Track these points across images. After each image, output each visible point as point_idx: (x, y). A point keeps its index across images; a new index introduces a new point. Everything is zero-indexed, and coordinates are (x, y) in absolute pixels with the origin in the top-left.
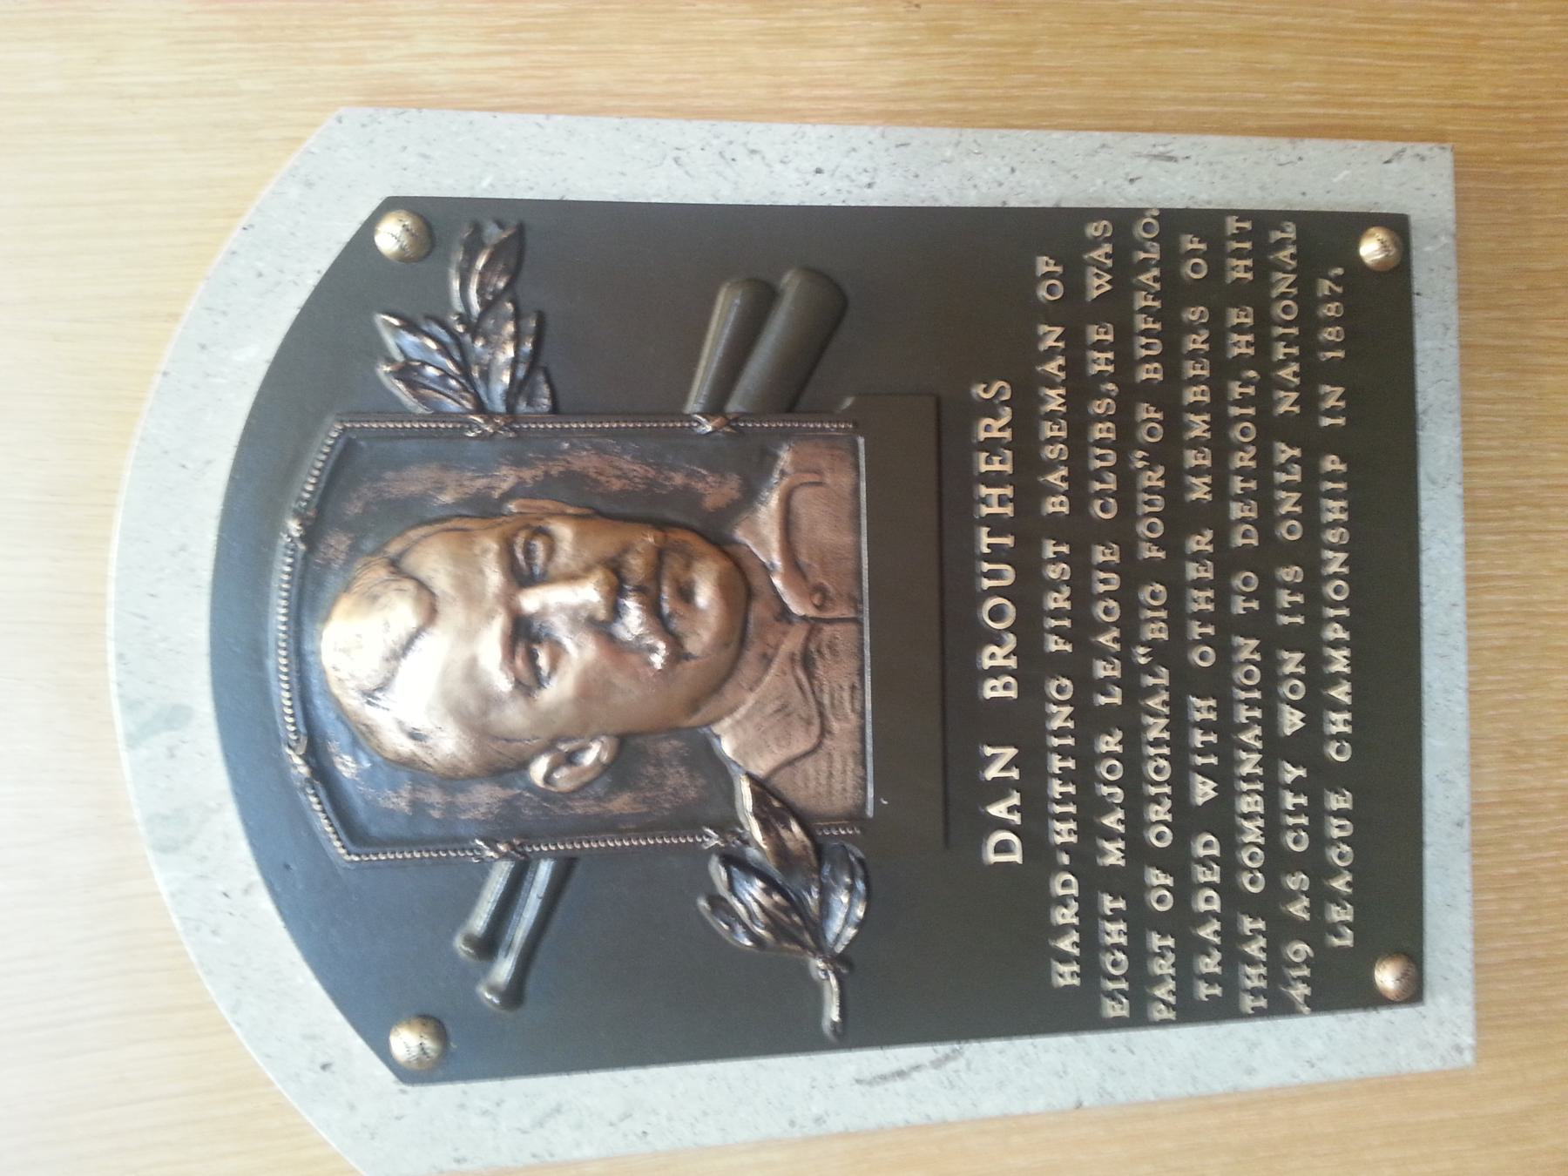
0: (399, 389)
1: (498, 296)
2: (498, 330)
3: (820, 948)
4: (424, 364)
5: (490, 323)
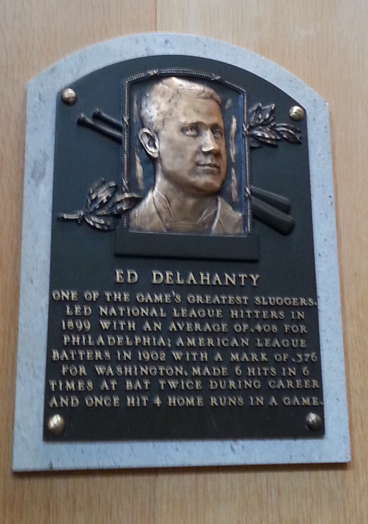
0: (255, 108)
1: (281, 136)
2: (273, 134)
4: (262, 114)
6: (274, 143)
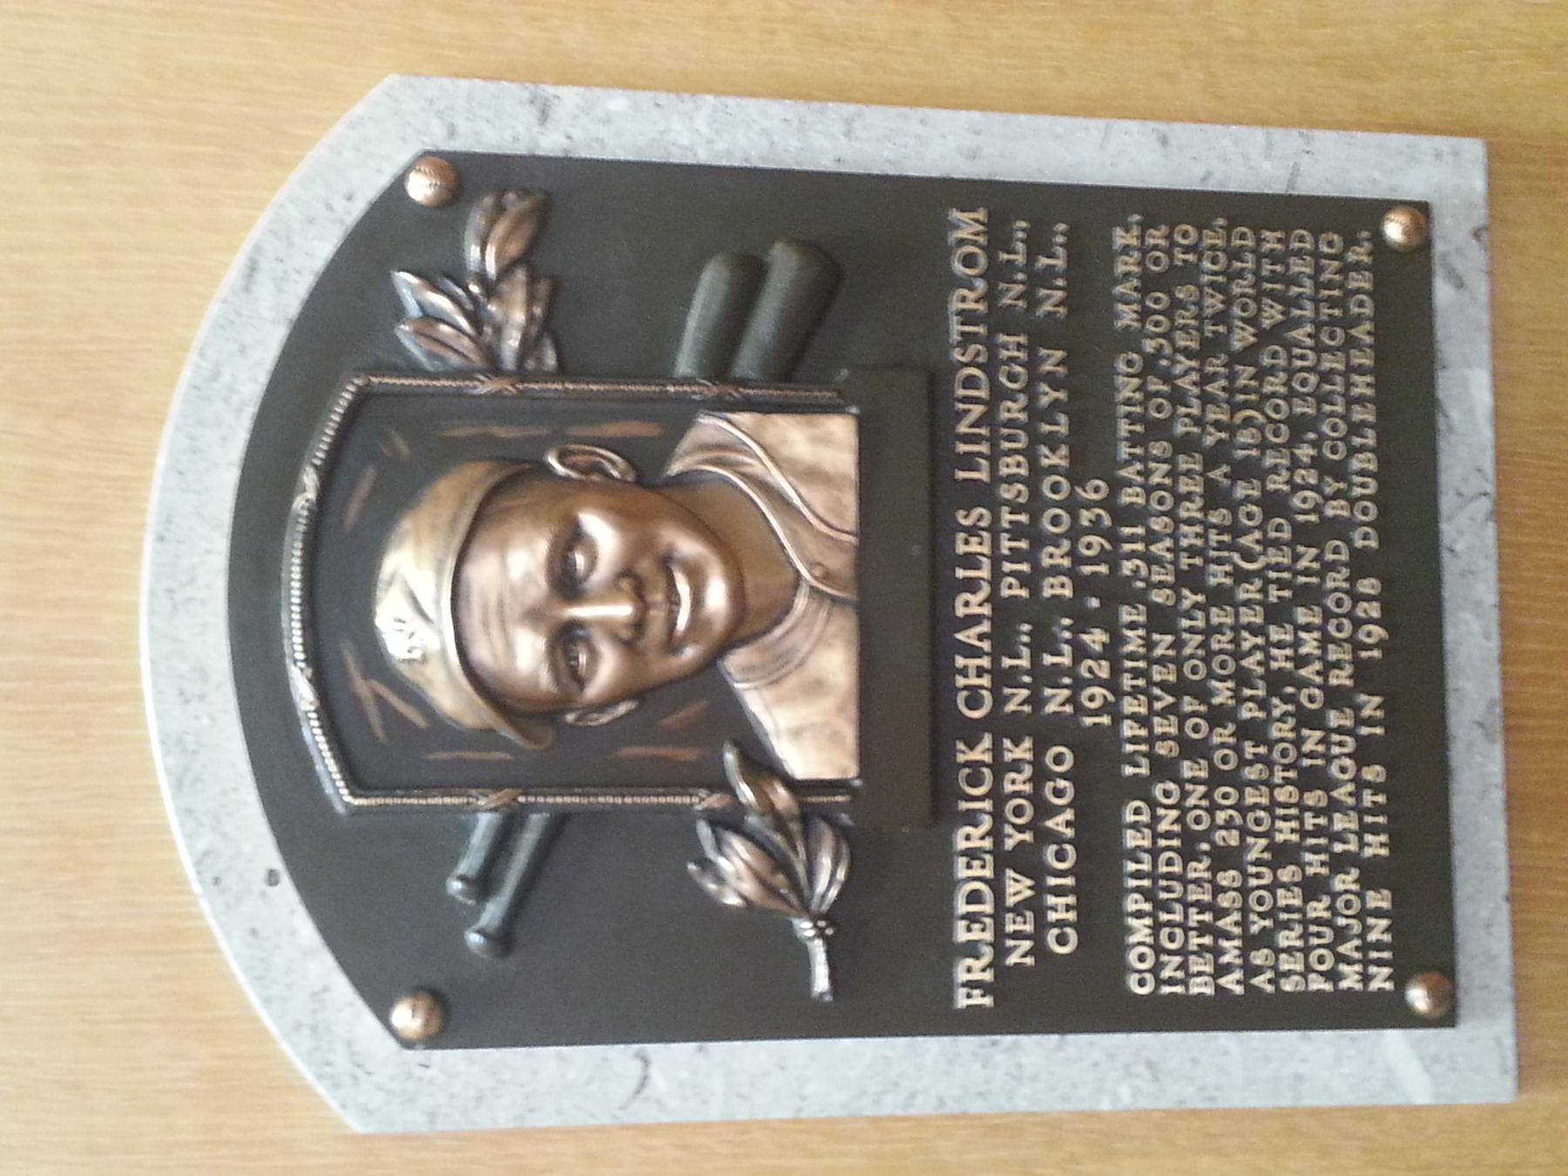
3: (805, 909)
5: (504, 287)
6: (543, 288)
